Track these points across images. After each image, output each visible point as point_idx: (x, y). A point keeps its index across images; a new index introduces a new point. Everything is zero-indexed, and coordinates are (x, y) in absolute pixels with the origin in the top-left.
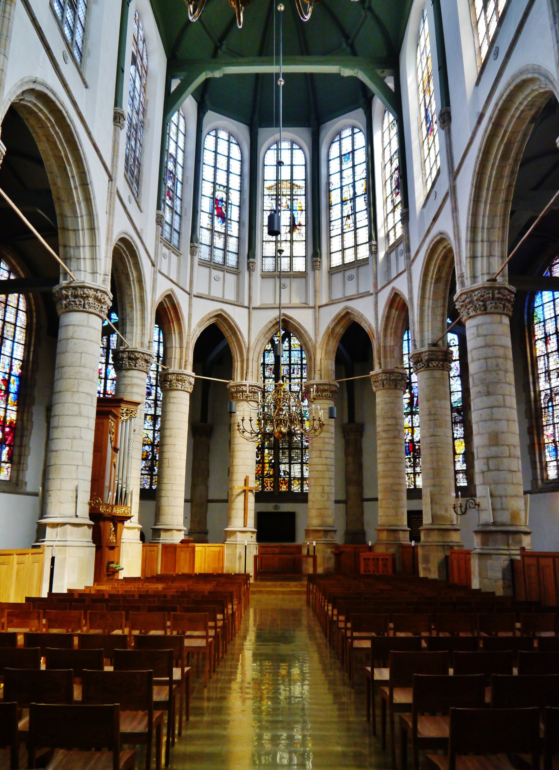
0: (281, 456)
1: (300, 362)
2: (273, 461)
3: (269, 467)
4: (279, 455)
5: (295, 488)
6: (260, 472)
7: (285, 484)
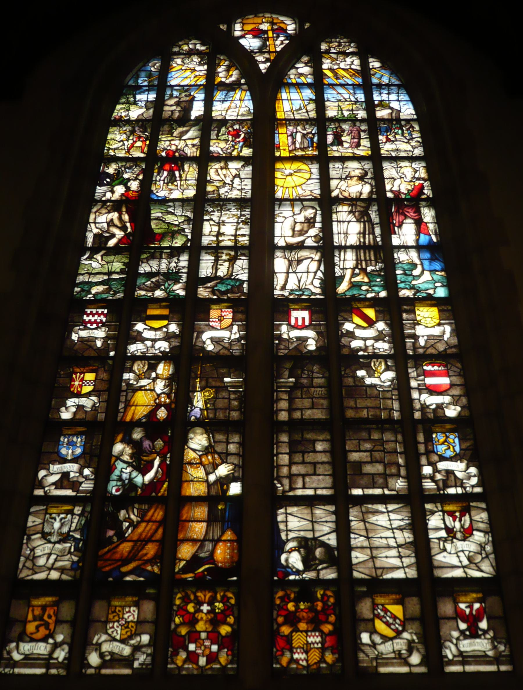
1: (362, 114)
2: (235, 489)
3: (210, 520)
5: (386, 648)
6: (151, 550)
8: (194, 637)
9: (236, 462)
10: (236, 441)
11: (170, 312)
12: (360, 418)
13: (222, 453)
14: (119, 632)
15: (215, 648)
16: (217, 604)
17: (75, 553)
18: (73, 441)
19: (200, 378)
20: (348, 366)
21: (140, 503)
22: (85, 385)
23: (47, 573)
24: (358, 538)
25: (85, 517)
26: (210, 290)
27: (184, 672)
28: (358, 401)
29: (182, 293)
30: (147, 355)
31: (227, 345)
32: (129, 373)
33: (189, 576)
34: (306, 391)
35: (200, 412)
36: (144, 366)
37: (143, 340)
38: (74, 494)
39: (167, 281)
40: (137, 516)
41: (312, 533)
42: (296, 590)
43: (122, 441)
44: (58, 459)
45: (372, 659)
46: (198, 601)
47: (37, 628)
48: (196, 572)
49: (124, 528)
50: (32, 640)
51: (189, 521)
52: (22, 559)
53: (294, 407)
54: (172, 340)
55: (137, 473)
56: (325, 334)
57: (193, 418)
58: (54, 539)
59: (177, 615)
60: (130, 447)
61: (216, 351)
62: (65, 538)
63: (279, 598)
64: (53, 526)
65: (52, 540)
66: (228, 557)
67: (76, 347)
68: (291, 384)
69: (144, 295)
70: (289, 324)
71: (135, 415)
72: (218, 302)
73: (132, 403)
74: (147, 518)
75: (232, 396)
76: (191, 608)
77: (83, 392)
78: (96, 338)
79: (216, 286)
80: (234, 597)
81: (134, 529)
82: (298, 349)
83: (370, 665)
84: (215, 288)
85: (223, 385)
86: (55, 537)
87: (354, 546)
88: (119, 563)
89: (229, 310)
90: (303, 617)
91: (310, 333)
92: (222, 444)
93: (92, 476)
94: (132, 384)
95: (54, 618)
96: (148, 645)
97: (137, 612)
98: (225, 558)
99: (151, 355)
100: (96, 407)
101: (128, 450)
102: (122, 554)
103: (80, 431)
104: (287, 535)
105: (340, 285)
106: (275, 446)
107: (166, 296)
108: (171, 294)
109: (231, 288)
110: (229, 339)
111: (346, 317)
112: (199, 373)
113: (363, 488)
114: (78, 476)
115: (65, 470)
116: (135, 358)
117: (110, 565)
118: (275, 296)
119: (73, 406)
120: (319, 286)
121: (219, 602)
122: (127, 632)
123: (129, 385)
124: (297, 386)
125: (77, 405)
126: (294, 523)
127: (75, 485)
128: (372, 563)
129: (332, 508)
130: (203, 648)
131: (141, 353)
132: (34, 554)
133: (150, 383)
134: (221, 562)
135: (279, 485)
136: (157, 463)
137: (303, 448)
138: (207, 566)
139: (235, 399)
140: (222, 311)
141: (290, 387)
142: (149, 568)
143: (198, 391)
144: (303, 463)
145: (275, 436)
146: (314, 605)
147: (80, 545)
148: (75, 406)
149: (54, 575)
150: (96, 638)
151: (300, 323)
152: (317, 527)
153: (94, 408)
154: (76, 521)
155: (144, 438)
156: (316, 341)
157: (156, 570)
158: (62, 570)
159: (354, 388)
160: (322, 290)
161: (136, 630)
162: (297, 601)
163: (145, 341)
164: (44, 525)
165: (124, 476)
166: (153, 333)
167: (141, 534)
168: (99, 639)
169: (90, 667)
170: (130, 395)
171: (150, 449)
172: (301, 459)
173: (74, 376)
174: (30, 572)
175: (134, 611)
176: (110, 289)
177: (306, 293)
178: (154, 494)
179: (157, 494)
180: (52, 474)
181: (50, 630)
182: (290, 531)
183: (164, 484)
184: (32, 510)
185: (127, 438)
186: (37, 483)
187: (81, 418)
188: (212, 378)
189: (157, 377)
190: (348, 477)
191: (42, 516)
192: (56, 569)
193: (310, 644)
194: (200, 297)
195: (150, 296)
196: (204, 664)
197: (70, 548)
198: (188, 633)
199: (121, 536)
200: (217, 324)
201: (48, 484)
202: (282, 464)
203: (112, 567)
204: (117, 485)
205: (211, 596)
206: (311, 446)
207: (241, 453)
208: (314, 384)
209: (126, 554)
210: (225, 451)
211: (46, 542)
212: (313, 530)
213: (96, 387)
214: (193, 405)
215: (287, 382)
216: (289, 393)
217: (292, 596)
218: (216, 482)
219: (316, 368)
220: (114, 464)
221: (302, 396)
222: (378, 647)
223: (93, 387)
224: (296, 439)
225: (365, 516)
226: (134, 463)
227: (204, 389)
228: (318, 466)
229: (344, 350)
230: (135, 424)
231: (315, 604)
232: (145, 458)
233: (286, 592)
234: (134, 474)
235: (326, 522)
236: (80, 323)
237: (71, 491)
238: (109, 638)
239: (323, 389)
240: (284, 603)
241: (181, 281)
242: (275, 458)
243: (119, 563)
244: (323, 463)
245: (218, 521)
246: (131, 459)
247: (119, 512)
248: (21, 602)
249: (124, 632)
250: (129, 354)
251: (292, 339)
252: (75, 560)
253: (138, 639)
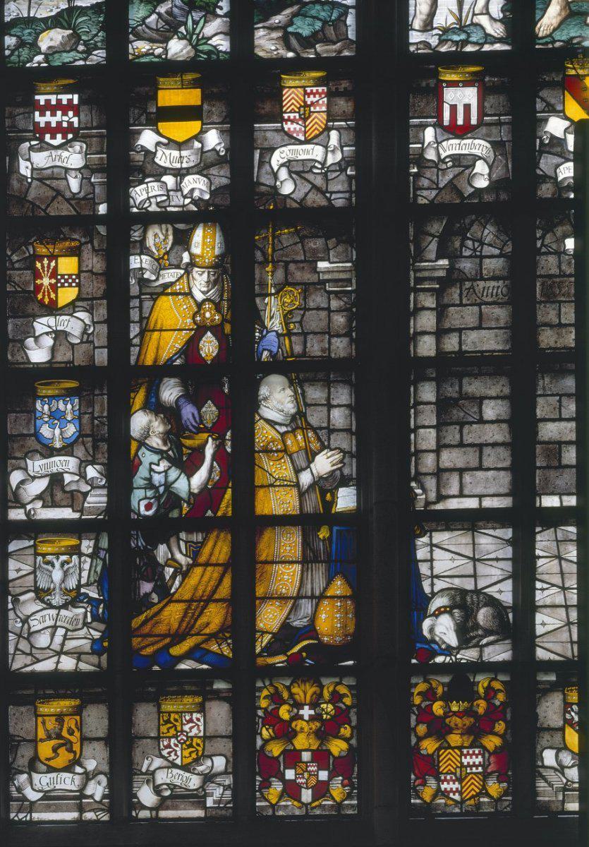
0: (428, 438)
2: (346, 499)
3: (308, 559)
4: (404, 432)
6: (214, 616)
7: (477, 731)
8: (293, 758)
9: (345, 446)
10: (345, 403)
11: (203, 99)
12: (564, 348)
13: (321, 428)
14: (179, 753)
15: (323, 775)
16: (324, 706)
17: (95, 624)
18: (58, 408)
19: (273, 261)
20: (549, 229)
21: (189, 531)
22: (63, 286)
23: (55, 659)
24: (547, 589)
25: (101, 559)
26: (280, 34)
27: (281, 813)
28: (563, 310)
29: (223, 44)
30: (169, 209)
31: (319, 181)
32: (140, 255)
33: (279, 660)
34: (469, 289)
35: (277, 340)
36: (166, 236)
37: (159, 173)
38: (76, 516)
39: (189, 12)
40: (186, 556)
41: (472, 580)
42: (446, 679)
43: (146, 407)
44: (39, 447)
45: (558, 790)
46: (294, 700)
47: (55, 750)
48: (289, 653)
49: (168, 578)
50: (51, 770)
51: (273, 562)
52: (12, 637)
53: (447, 325)
54: (214, 171)
55: (178, 472)
56: (508, 147)
57: (266, 353)
58: (57, 600)
59: (264, 725)
60: (159, 420)
61: (298, 196)
62: (75, 598)
63: (419, 694)
64: (51, 576)
65: (54, 603)
66: (339, 625)
67: (32, 195)
68: (442, 274)
69: (147, 54)
70: (439, 124)
71: (160, 352)
72: (297, 66)
73: (152, 327)
74: (202, 559)
75: (335, 304)
76: (284, 713)
77: (61, 303)
78: (67, 170)
79: (291, 23)
80: (349, 695)
81: (183, 579)
82: (455, 186)
83: (554, 799)
84: (290, 29)
85: (314, 278)
86: (57, 597)
87: (540, 603)
88: (167, 640)
89: (320, 89)
90: (456, 725)
91: (478, 146)
92: (320, 408)
93: (102, 479)
94: (148, 281)
95: (77, 734)
96: (225, 772)
97: (202, 720)
98: (333, 627)
99: (176, 209)
100: (89, 335)
101: (158, 427)
102: (169, 624)
103: (66, 389)
104: (432, 585)
105: (545, 10)
106: (412, 411)
107: (192, 54)
108: (201, 48)
109: (322, 29)
110: (323, 164)
111: (553, 101)
112: (270, 250)
113: (560, 495)
114: (78, 481)
115: (55, 470)
116: (148, 219)
117: (153, 644)
118: (412, 49)
119: (47, 333)
120: (501, 15)
121: (327, 703)
122: (190, 753)
123: (143, 282)
124: (452, 278)
125: (55, 332)
126: (443, 563)
127: (74, 499)
128: (568, 634)
129: (508, 533)
130: (306, 775)
131: (158, 204)
132: (29, 628)
133: (182, 276)
134: (328, 636)
135: (419, 491)
136: (209, 451)
137: (462, 414)
138: (305, 643)
139: (339, 311)
140: (305, 93)
141: (439, 280)
142: (214, 648)
143: (271, 295)
144: (461, 445)
145: (412, 389)
146: (472, 705)
147: (101, 610)
148: (50, 332)
149: (68, 664)
150: (146, 763)
151: (460, 122)
152: (482, 569)
153: (85, 337)
154: (87, 566)
155: (183, 400)
156: (490, 167)
157: (227, 651)
158: (78, 655)
159: (558, 280)
160: (507, 29)
161: (204, 749)
162: (447, 698)
163: (162, 175)
164: (36, 577)
165: (158, 479)
166: (175, 153)
167: (196, 589)
168: (150, 765)
169: (144, 807)
170: (147, 304)
171: (194, 424)
172: (458, 437)
173: (38, 265)
174: (28, 660)
175: (198, 720)
176: (76, 37)
177: (473, 39)
178: (209, 513)
179: (215, 512)
180: (34, 478)
181: (75, 753)
182: (438, 577)
183: (225, 493)
184: (12, 547)
185: (153, 400)
186: (10, 496)
187: (65, 360)
188: (296, 262)
189: (192, 264)
190: (538, 471)
191: (30, 560)
192: (66, 653)
193: (466, 767)
194: (261, 54)
195: (159, 56)
196: (310, 800)
197: (85, 616)
198: (283, 752)
199: (163, 590)
200: (298, 127)
201: (30, 499)
202: (424, 448)
203: (155, 647)
204: (146, 498)
205: (315, 693)
206: (476, 409)
207: (354, 428)
208: (484, 272)
209: (175, 625)
210: (325, 425)
211: (45, 606)
212: (475, 576)
213: (83, 290)
214: (265, 327)
215: (434, 269)
216: (439, 294)
217: (440, 691)
218: (312, 486)
219: (489, 233)
220: (136, 454)
221: (461, 300)
222: (566, 771)
223: (77, 289)
224: (449, 395)
225: (562, 549)
226: (170, 453)
227: (281, 290)
228: (487, 451)
229: (544, 187)
230: (161, 371)
231: (475, 703)
232: (188, 442)
233: (431, 684)
234: (174, 473)
235: (497, 559)
236: (30, 131)
237: (70, 510)
238: (165, 763)
239: (501, 283)
240: (428, 703)
241: (219, 12)
242: (412, 436)
243: (167, 640)
244: (494, 445)
245: (319, 562)
246: (165, 443)
247: (156, 548)
248: (23, 709)
249: (186, 753)
250: (135, 210)
251: (443, 161)
252: (95, 637)
253: (209, 763)
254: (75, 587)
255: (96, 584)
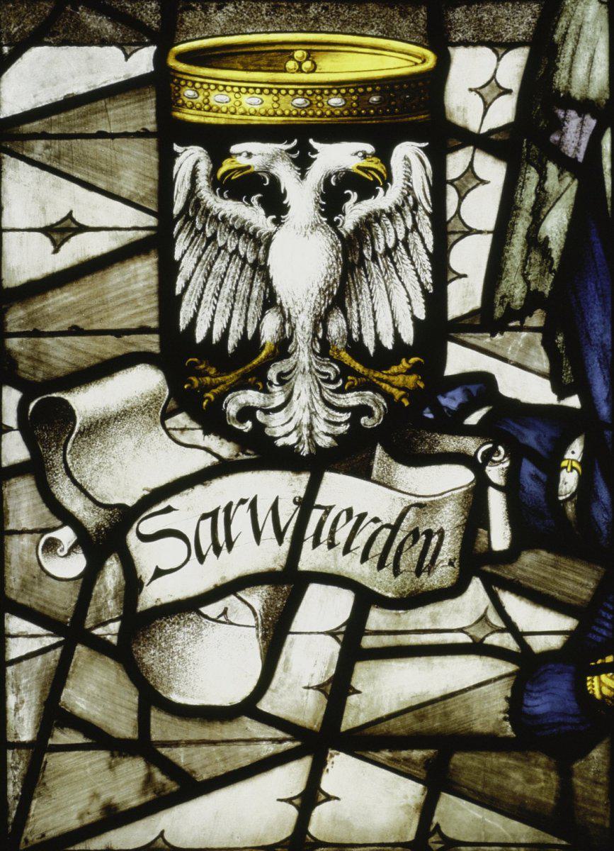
17: (531, 563)
25: (566, 164)
64: (261, 268)
86: (303, 387)
147: (569, 481)
252: (539, 644)
254: (408, 336)
255: (536, 320)
